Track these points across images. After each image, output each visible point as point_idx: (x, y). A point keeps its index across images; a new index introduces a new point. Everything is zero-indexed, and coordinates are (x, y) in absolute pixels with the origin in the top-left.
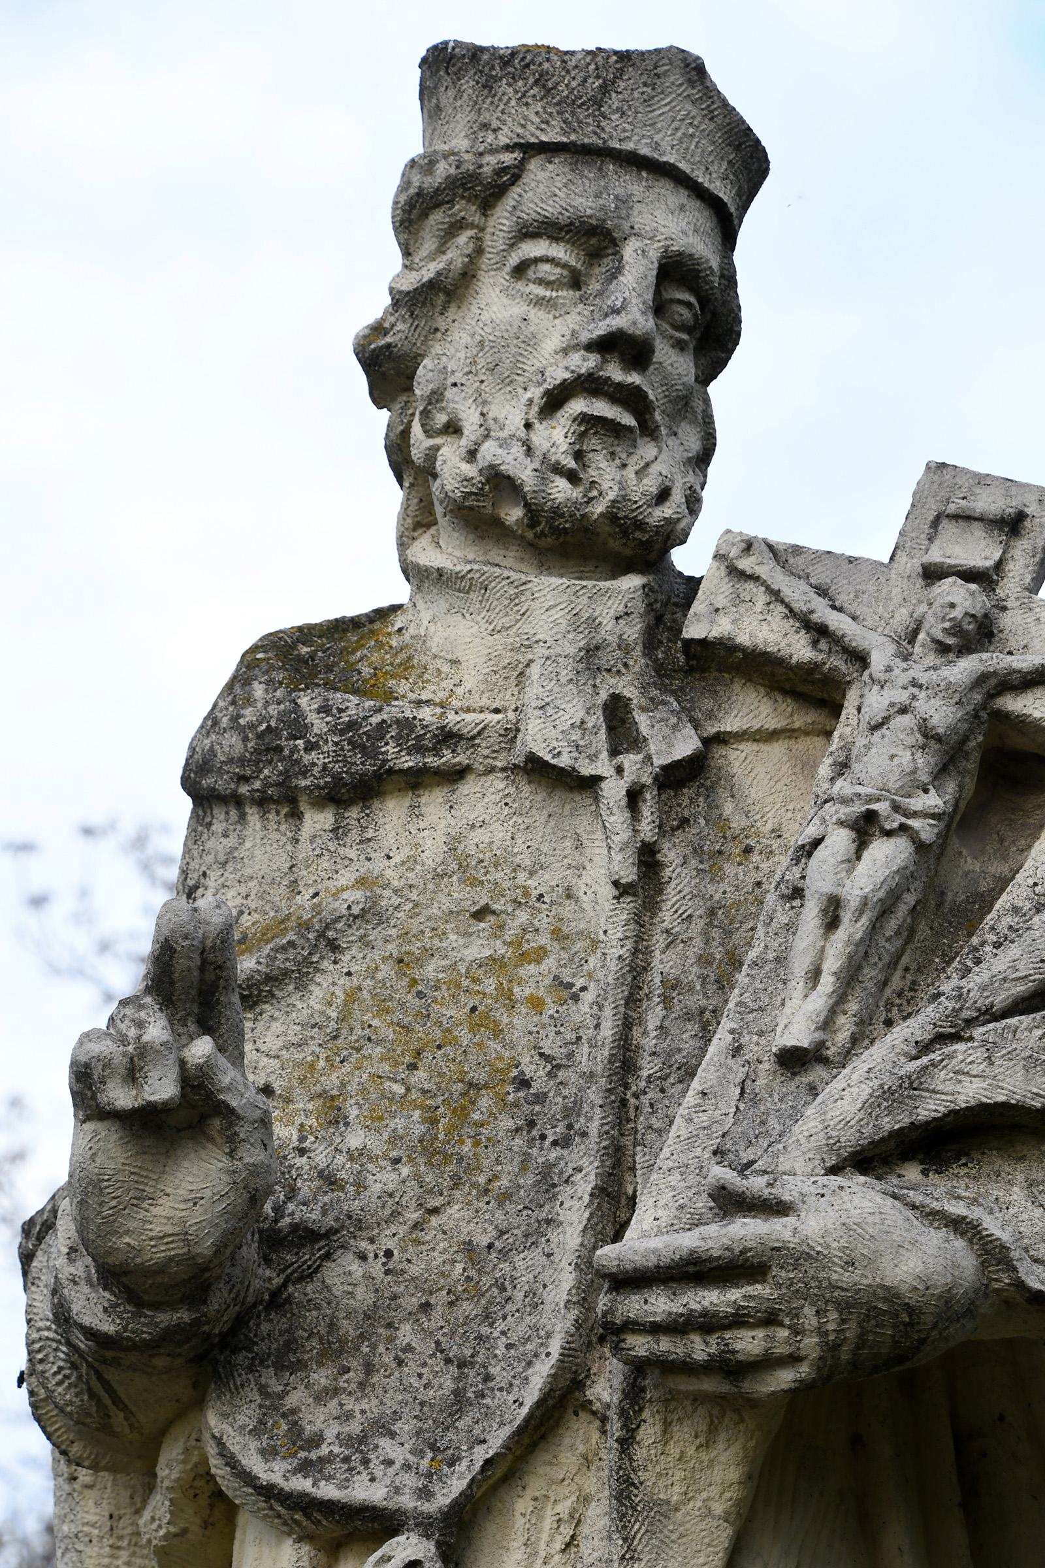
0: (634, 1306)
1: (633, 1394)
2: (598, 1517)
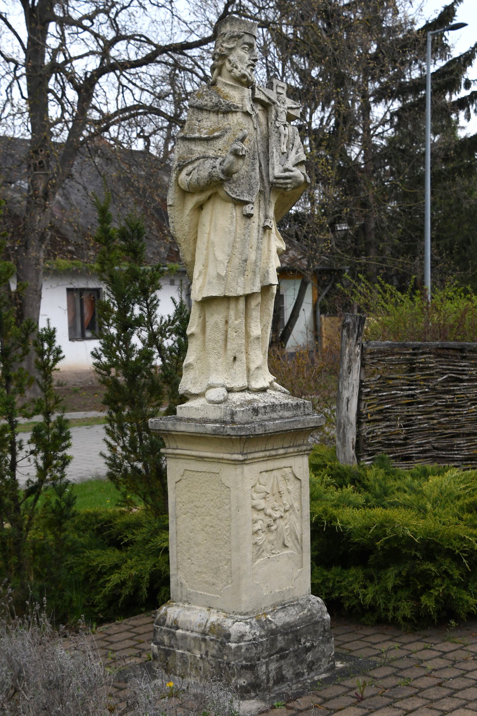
0: (279, 181)
2: (262, 203)
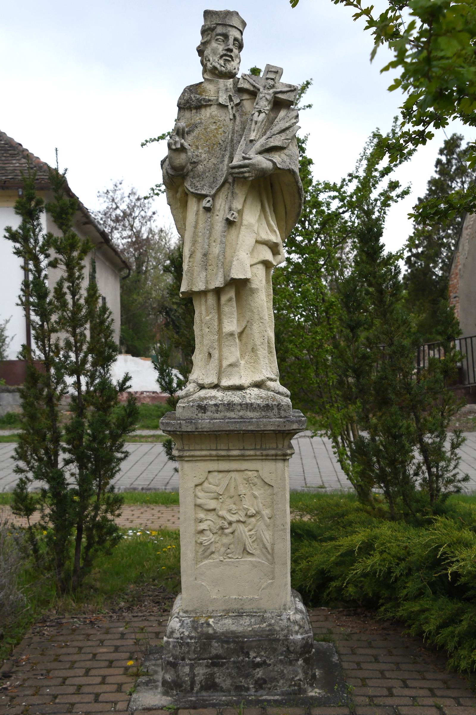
0: (233, 171)
1: (234, 181)
2: (230, 195)
